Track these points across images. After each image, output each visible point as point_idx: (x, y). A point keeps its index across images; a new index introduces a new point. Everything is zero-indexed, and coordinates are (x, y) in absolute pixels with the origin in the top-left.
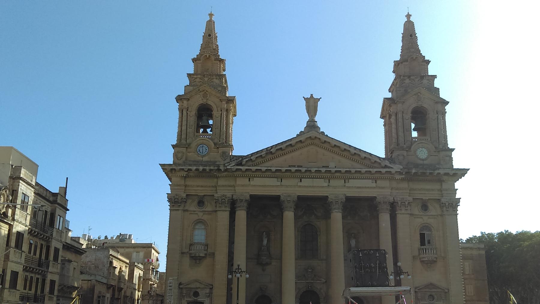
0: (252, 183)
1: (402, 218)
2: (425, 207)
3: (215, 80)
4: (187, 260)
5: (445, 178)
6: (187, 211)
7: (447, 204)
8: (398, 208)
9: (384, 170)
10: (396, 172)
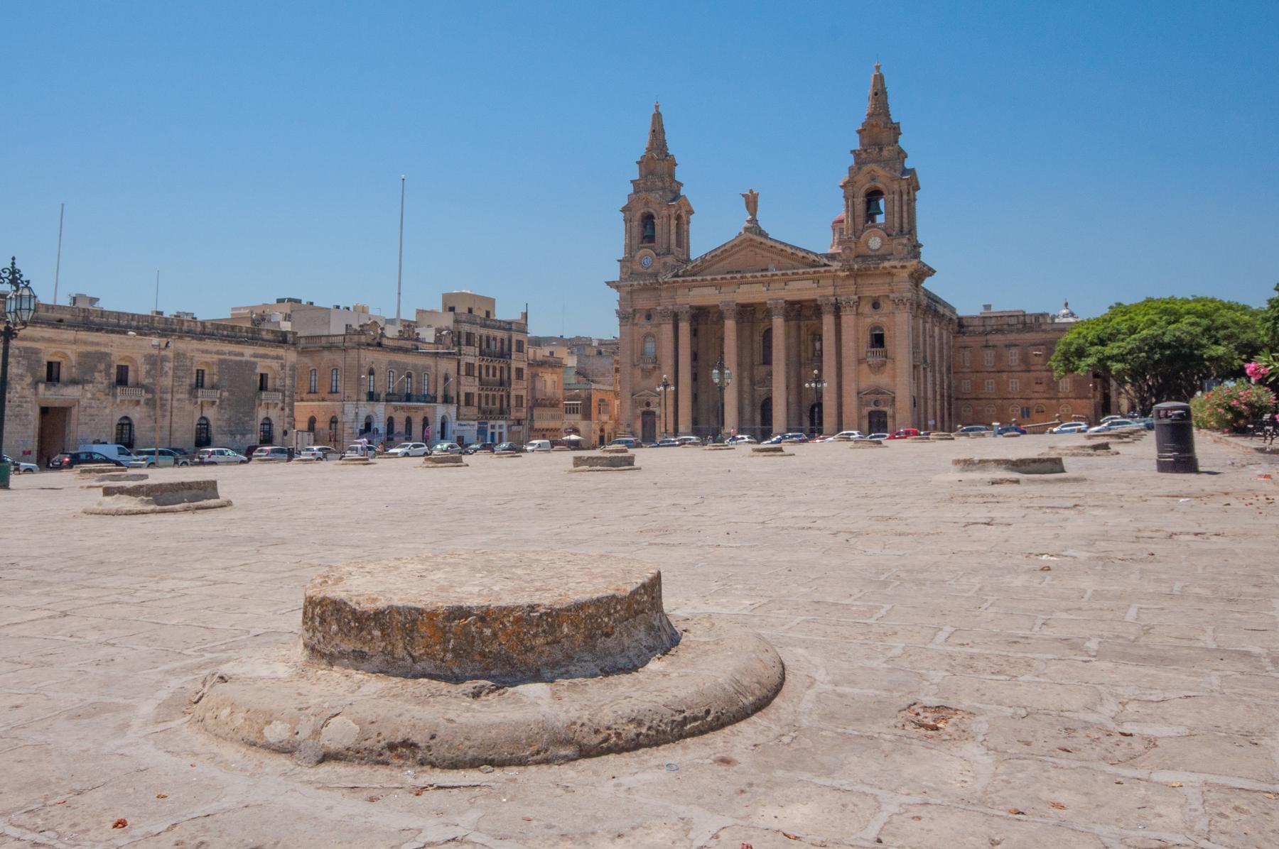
1: (848, 319)
2: (876, 305)
4: (638, 373)
5: (894, 270)
6: (636, 324)
7: (897, 301)
8: (842, 309)
9: (822, 269)
10: (836, 271)
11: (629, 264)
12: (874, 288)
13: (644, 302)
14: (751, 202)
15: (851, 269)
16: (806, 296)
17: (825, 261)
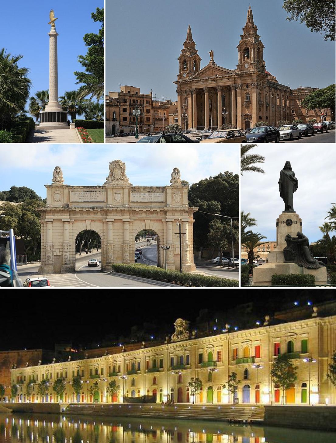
1: (239, 91)
2: (247, 87)
9: (230, 75)
10: (234, 75)
12: (246, 81)
16: (227, 84)
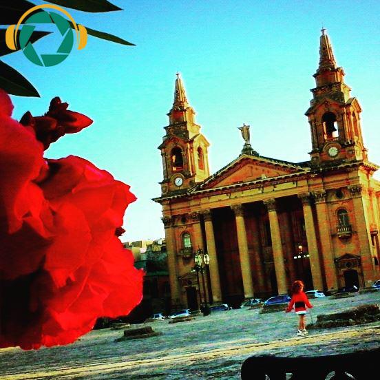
0: (210, 200)
1: (321, 207)
3: (182, 127)
4: (181, 262)
6: (176, 226)
9: (298, 174)
11: (166, 185)
13: (179, 209)
14: (245, 132)
15: (318, 172)
16: (289, 193)
17: (299, 168)
